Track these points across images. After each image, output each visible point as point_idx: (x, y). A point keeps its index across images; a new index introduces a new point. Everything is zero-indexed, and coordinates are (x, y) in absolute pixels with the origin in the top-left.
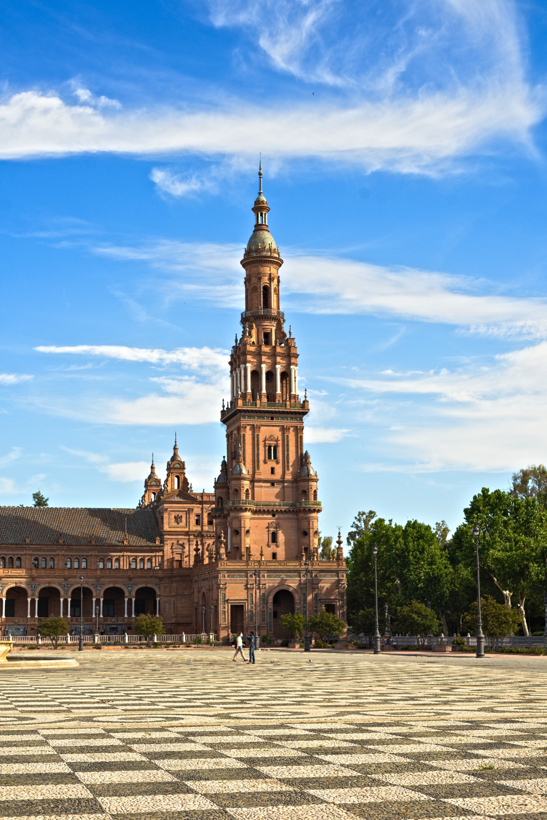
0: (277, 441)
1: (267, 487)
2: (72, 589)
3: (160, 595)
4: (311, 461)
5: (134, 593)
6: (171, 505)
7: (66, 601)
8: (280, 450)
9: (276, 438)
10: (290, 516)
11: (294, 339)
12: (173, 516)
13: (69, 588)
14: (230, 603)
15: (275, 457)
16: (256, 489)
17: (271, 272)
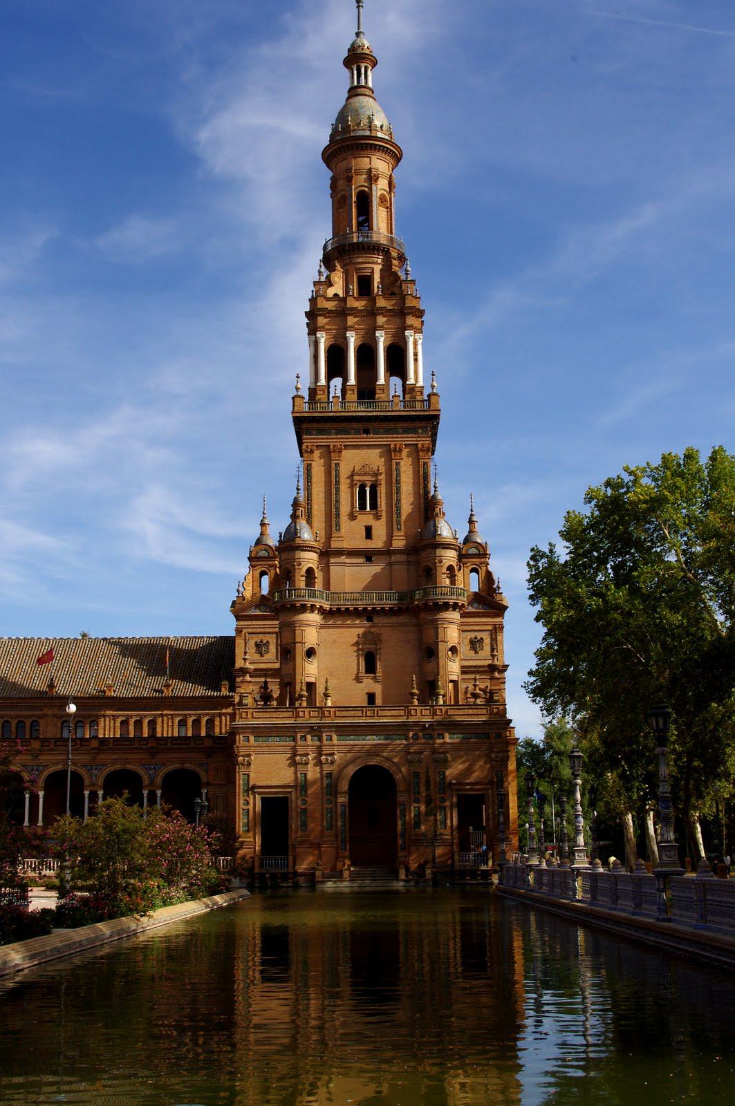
0: (376, 474)
1: (356, 564)
2: (45, 774)
3: (208, 784)
4: (444, 510)
5: (159, 781)
6: (249, 623)
7: (34, 798)
8: (382, 491)
9: (375, 469)
10: (403, 619)
11: (413, 282)
12: (252, 643)
13: (41, 773)
14: (259, 793)
15: (374, 506)
16: (334, 570)
17: (373, 165)
